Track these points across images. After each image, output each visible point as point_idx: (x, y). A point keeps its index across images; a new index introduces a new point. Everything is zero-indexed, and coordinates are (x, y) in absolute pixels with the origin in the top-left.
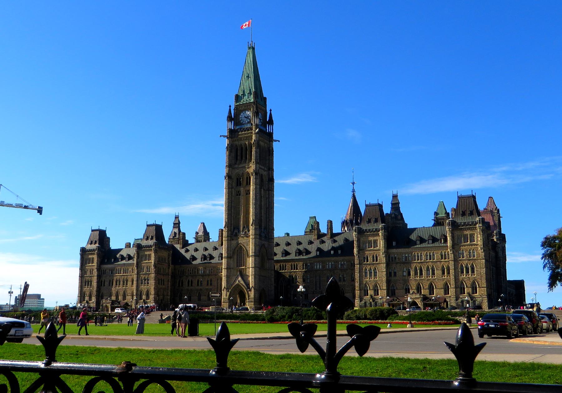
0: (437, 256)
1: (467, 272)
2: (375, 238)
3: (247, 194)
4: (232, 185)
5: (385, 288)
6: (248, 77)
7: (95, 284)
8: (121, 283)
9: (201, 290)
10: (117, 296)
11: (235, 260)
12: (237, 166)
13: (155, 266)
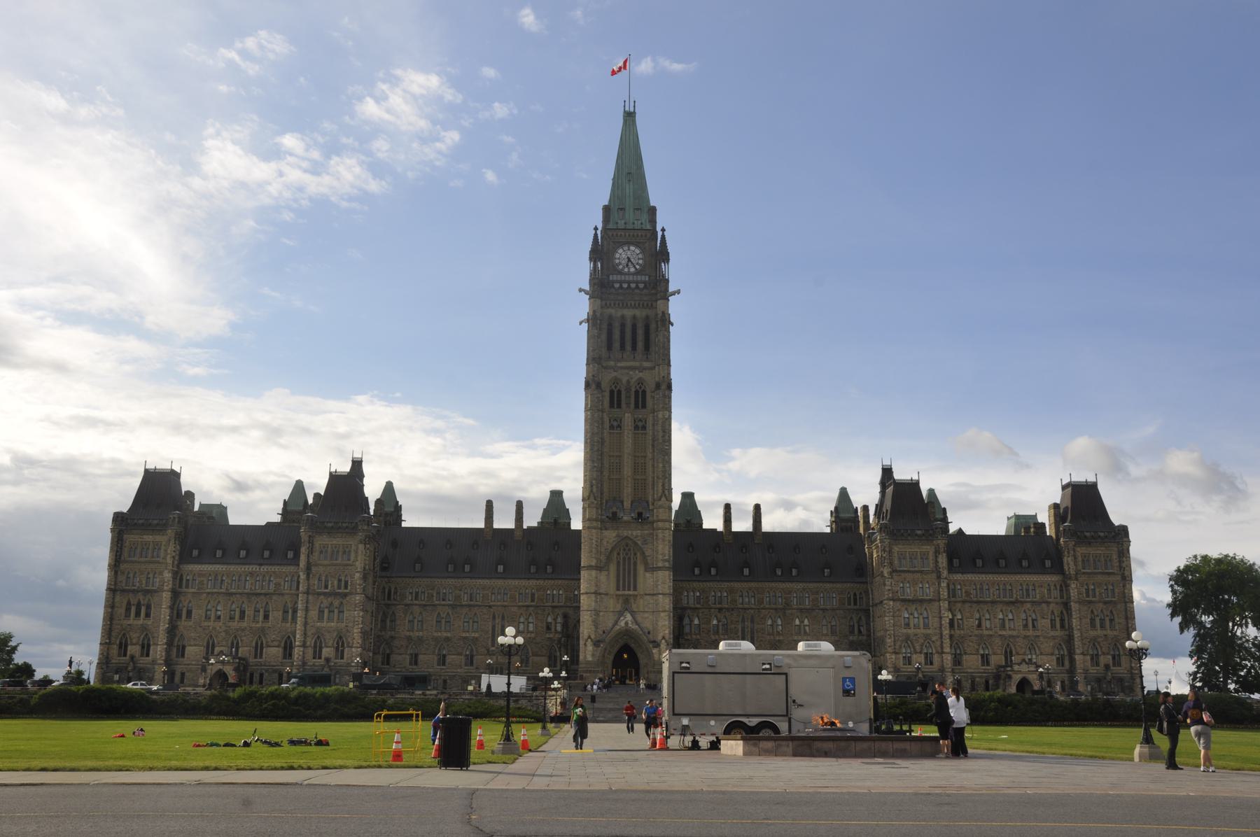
1: (1102, 627)
3: (636, 427)
5: (947, 650)
7: (163, 613)
8: (249, 612)
9: (447, 639)
12: (612, 363)
13: (365, 578)
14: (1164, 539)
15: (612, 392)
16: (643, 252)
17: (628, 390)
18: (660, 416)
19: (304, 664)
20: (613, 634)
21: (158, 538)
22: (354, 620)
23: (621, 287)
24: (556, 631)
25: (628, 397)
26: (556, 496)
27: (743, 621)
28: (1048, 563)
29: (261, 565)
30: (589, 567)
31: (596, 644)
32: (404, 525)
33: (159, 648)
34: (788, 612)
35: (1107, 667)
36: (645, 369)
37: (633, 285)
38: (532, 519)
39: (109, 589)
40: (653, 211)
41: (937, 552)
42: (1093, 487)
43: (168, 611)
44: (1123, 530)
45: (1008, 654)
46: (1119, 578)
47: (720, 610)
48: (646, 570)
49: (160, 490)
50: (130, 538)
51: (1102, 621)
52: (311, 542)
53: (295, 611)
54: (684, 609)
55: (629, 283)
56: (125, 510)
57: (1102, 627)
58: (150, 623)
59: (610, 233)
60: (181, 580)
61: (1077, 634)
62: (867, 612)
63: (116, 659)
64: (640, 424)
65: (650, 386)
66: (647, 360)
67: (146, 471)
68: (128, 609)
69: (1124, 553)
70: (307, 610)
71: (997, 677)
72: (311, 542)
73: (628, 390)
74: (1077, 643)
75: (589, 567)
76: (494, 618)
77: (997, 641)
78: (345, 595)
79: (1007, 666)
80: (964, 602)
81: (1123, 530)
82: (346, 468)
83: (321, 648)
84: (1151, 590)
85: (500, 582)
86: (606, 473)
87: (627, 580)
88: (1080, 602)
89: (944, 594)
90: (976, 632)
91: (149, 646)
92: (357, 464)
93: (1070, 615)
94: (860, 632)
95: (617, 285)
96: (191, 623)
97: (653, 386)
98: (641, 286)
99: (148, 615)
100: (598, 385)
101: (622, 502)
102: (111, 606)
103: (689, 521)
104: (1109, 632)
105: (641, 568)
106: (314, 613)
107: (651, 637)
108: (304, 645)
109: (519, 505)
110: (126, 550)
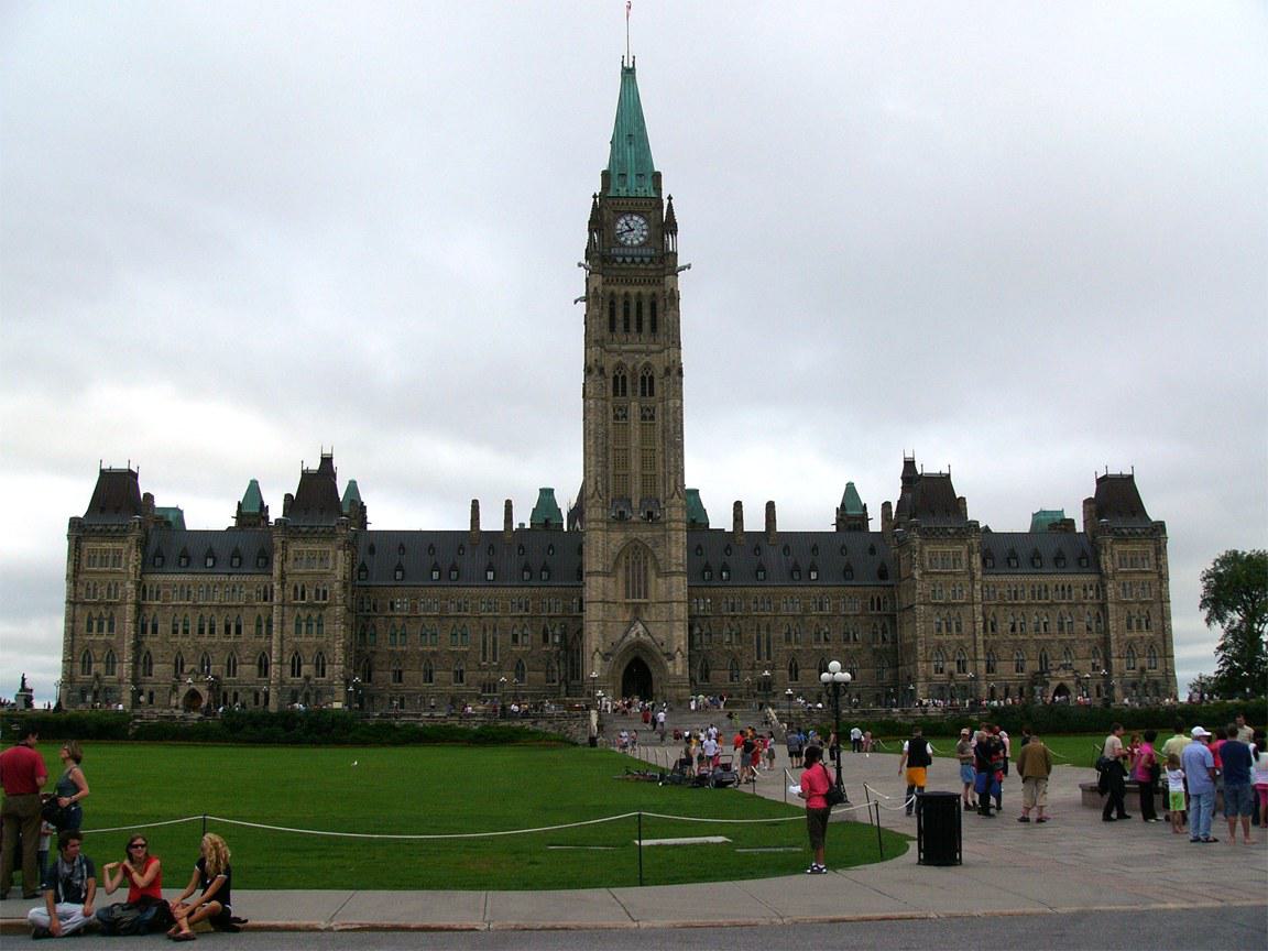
0: (1078, 594)
1: (1139, 627)
2: (959, 548)
3: (644, 418)
5: (981, 656)
6: (630, 136)
7: (129, 628)
8: (220, 627)
9: (433, 653)
10: (205, 662)
11: (621, 582)
13: (345, 586)
14: (1199, 531)
15: (616, 378)
16: (647, 221)
17: (634, 375)
18: (671, 404)
19: (282, 682)
20: (623, 646)
21: (118, 546)
22: (336, 635)
23: (624, 261)
24: (554, 643)
25: (634, 384)
26: (547, 494)
27: (758, 630)
28: (1084, 562)
29: (230, 574)
30: (597, 573)
31: (605, 657)
32: (369, 528)
33: (125, 666)
34: (807, 619)
35: (1143, 670)
36: (652, 352)
37: (637, 260)
38: (522, 517)
39: (68, 602)
40: (657, 176)
41: (970, 552)
42: (1131, 477)
43: (132, 625)
44: (1160, 526)
45: (1044, 660)
46: (1156, 577)
47: (734, 617)
48: (658, 577)
49: (117, 493)
50: (87, 546)
51: (1139, 621)
52: (285, 548)
53: (270, 626)
54: (695, 617)
55: (633, 257)
56: (82, 516)
57: (1139, 627)
58: (113, 639)
59: (610, 202)
60: (144, 591)
61: (1113, 636)
62: (892, 618)
63: (81, 677)
64: (648, 414)
65: (659, 370)
66: (654, 343)
67: (102, 471)
68: (90, 623)
69: (1160, 551)
70: (283, 623)
71: (1033, 683)
72: (285, 548)
73: (634, 375)
74: (1113, 646)
75: (597, 573)
76: (485, 630)
77: (1033, 647)
78: (325, 606)
79: (1042, 673)
80: (998, 605)
81: (1160, 527)
82: (315, 465)
83: (299, 666)
84: (1186, 582)
85: (490, 591)
86: (611, 467)
87: (637, 586)
88: (1119, 603)
89: (978, 597)
90: (1011, 637)
91: (114, 663)
92: (327, 461)
93: (1107, 617)
94: (884, 639)
95: (620, 260)
96: (156, 639)
97: (662, 371)
98: (647, 260)
99: (111, 629)
100: (602, 371)
101: (630, 501)
102: (71, 620)
103: (694, 521)
104: (1147, 635)
105: (652, 574)
106: (290, 627)
107: (665, 649)
108: (281, 663)
109: (508, 505)
110: (84, 558)
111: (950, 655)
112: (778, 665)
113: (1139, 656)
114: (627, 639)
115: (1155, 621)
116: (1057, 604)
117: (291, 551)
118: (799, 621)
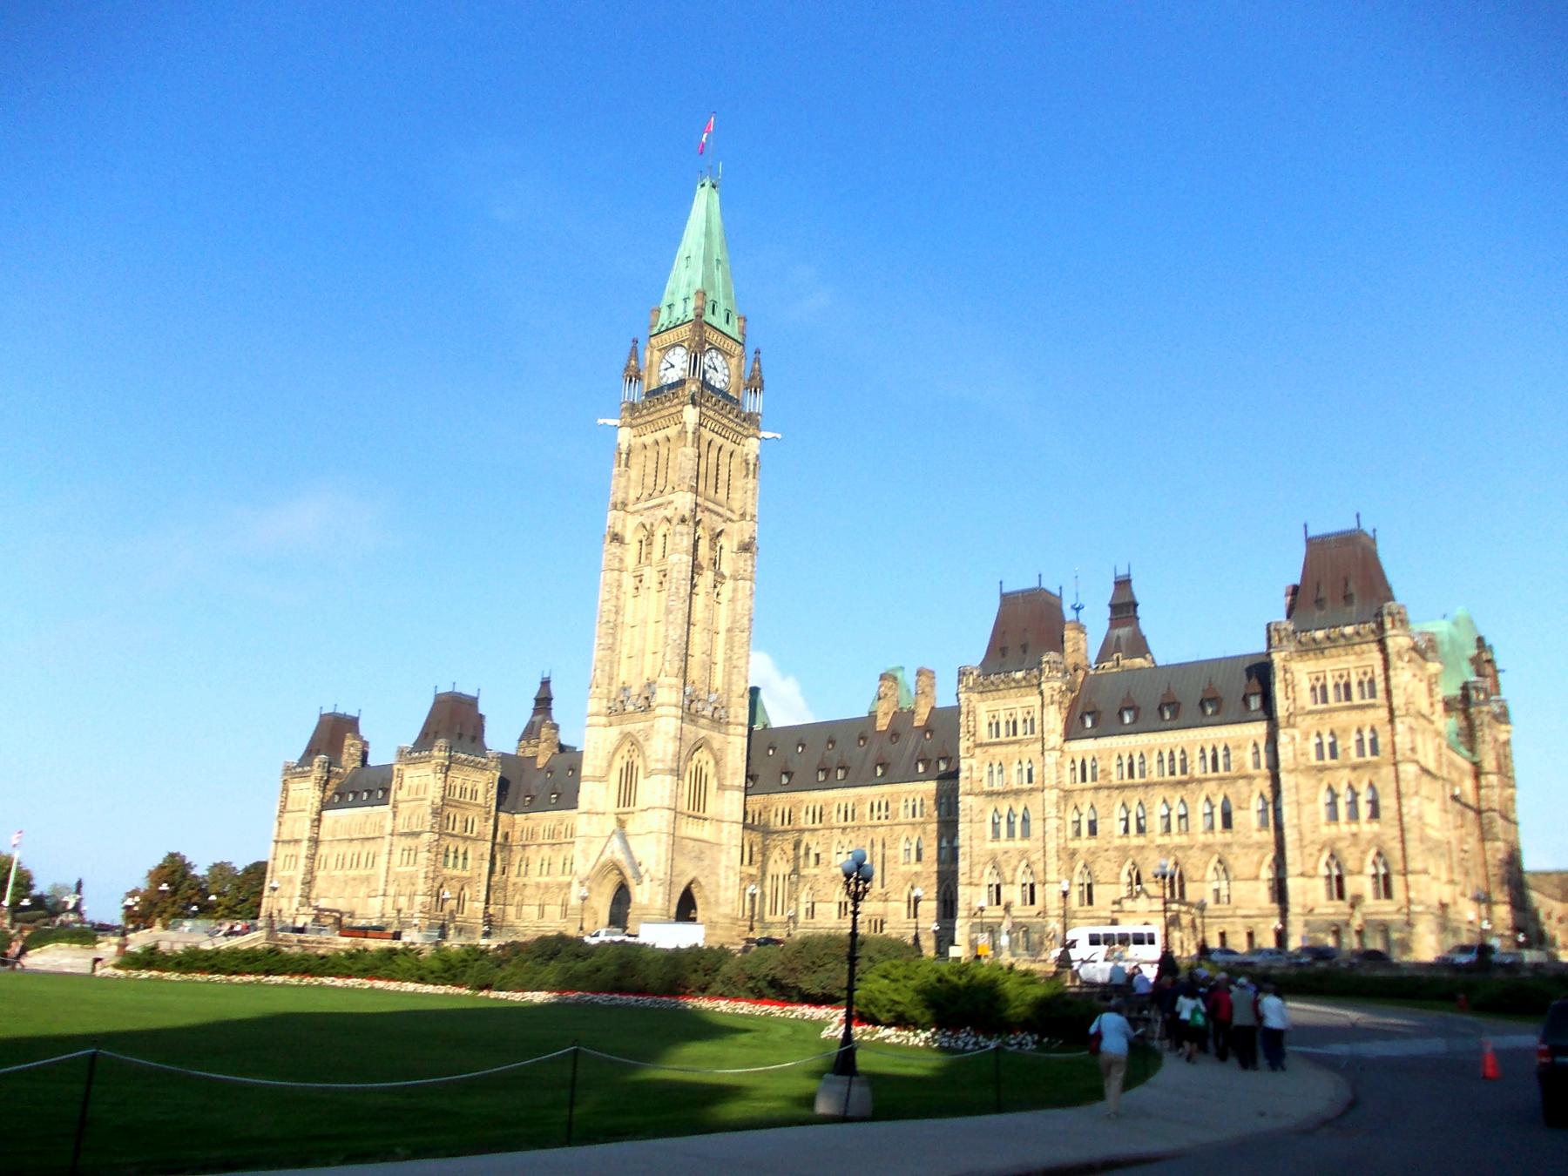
4: (621, 560)
46: (1383, 713)
47: (844, 829)
54: (802, 831)
61: (1290, 835)
80: (1097, 789)
92: (546, 683)
111: (1008, 877)
112: (892, 896)
113: (1351, 873)
114: (603, 859)
115: (1387, 802)
116: (1200, 781)
117: (407, 781)
118: (919, 831)
